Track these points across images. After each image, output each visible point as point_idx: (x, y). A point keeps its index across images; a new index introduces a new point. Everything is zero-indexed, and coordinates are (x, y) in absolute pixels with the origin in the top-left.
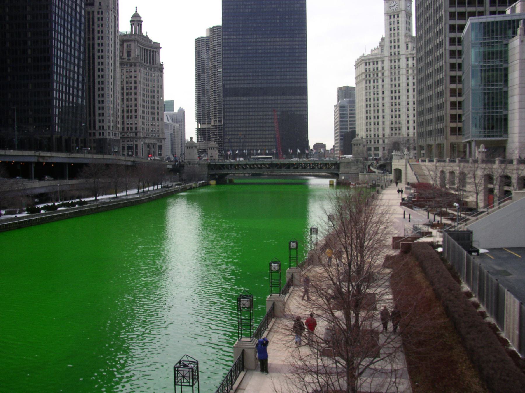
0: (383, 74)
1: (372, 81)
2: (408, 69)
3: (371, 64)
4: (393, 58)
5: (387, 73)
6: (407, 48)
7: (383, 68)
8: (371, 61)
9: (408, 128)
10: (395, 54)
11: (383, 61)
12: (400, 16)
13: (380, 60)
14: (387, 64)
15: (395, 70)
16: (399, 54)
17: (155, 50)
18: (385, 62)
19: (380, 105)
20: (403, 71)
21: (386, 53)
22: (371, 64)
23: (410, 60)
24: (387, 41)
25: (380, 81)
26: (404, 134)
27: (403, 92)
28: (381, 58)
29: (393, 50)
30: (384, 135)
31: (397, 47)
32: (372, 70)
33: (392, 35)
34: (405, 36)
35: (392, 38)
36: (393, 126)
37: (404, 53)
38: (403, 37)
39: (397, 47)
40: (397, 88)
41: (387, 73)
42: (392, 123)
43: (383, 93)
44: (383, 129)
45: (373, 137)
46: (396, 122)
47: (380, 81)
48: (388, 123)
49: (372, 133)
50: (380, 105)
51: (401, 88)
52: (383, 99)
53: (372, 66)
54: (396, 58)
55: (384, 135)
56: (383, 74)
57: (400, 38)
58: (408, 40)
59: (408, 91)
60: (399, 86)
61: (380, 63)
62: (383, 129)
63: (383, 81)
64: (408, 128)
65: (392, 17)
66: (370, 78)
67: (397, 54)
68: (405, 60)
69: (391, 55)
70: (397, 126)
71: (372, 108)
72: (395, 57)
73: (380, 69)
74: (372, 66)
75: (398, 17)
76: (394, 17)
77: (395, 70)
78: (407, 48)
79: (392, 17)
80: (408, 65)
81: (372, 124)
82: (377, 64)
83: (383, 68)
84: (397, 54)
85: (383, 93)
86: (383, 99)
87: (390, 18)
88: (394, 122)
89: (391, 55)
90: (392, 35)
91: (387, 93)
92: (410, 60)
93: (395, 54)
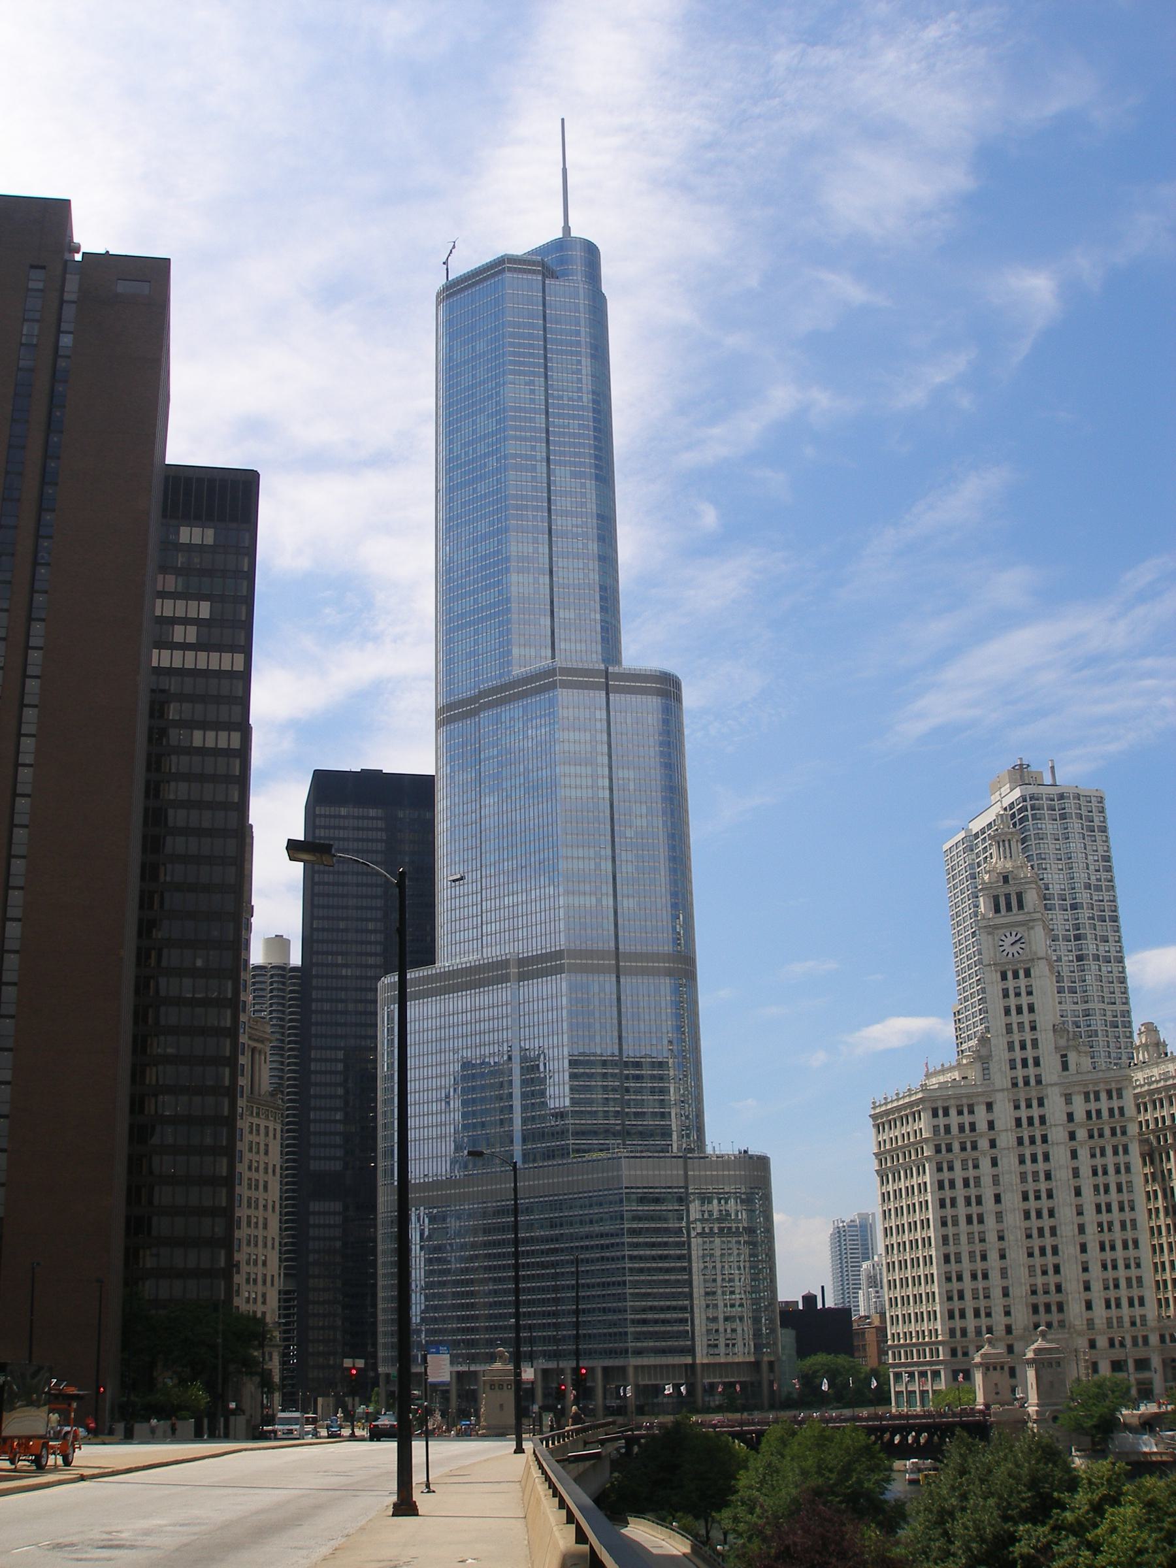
2: (1071, 1127)
3: (953, 1112)
5: (1006, 1139)
6: (1065, 1067)
9: (1089, 1306)
10: (1027, 1083)
11: (989, 1106)
14: (1004, 1114)
15: (1032, 1134)
17: (259, 1045)
20: (1058, 1134)
21: (1001, 1077)
23: (1078, 1100)
24: (999, 1044)
25: (985, 1163)
26: (1077, 1323)
27: (1064, 1201)
29: (1020, 1072)
30: (1009, 1330)
31: (1030, 1062)
33: (1015, 1027)
34: (1054, 1031)
35: (1016, 1038)
36: (1041, 1299)
37: (1054, 1078)
39: (1030, 1062)
40: (1043, 1186)
41: (1006, 1139)
42: (1034, 1292)
43: (998, 1199)
47: (985, 1163)
48: (1020, 1291)
51: (1052, 1184)
52: (999, 1216)
53: (954, 1120)
54: (1034, 1094)
56: (993, 1144)
58: (1062, 1042)
59: (1078, 1193)
60: (1048, 1176)
61: (981, 1110)
63: (994, 1163)
64: (1089, 1306)
65: (1010, 975)
67: (1033, 1082)
69: (1015, 1085)
70: (1054, 1298)
71: (965, 1249)
72: (1028, 1090)
73: (982, 1126)
74: (954, 1120)
75: (1028, 974)
76: (1016, 976)
77: (1032, 1134)
78: (1065, 1067)
79: (1010, 975)
80: (1070, 1117)
84: (1033, 1082)
85: (998, 1199)
86: (999, 1216)
87: (1004, 977)
89: (1015, 1085)
90: (1015, 1027)
91: (1012, 1200)
92: (1078, 1100)
93: (1027, 1083)
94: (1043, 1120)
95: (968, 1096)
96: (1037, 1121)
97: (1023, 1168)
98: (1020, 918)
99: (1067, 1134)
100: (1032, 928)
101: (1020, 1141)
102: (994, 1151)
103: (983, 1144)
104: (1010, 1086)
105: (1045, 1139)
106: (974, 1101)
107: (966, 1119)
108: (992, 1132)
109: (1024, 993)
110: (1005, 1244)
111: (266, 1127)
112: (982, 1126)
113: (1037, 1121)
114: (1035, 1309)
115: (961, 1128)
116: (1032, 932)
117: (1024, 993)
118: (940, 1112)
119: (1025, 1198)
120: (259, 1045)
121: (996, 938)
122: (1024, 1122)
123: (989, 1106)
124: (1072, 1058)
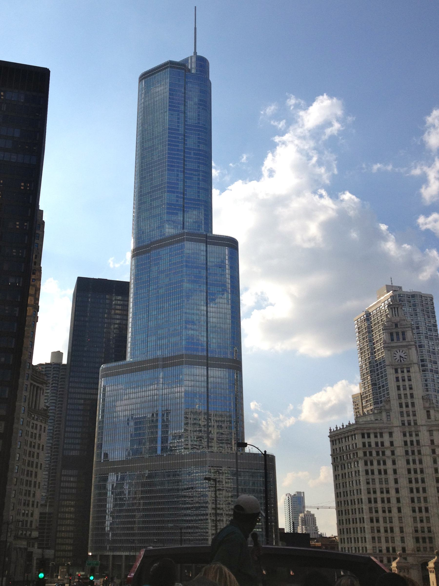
0: (393, 453)
1: (375, 463)
3: (372, 436)
4: (407, 430)
5: (400, 451)
7: (392, 443)
8: (372, 431)
10: (409, 424)
11: (391, 434)
12: (412, 370)
13: (386, 430)
14: (398, 439)
16: (416, 424)
17: (40, 386)
18: (394, 435)
19: (393, 501)
22: (372, 436)
25: (389, 463)
28: (387, 428)
32: (373, 445)
36: (420, 535)
37: (424, 423)
38: (421, 401)
41: (400, 451)
42: (416, 531)
44: (403, 540)
45: (384, 551)
46: (423, 528)
48: (409, 530)
49: (384, 546)
50: (393, 501)
53: (373, 440)
55: (404, 549)
56: (393, 453)
57: (416, 401)
60: (422, 471)
62: (403, 540)
63: (394, 463)
66: (371, 458)
67: (412, 424)
68: (427, 434)
69: (403, 424)
70: (426, 535)
73: (387, 444)
74: (373, 440)
81: (382, 530)
82: (381, 436)
83: (392, 443)
84: (412, 424)
87: (396, 371)
88: (419, 529)
89: (403, 424)
93: (409, 424)
94: (418, 442)
95: (381, 428)
96: (415, 443)
97: (409, 467)
98: (405, 344)
99: (431, 451)
100: (410, 349)
101: (407, 452)
102: (393, 457)
103: (388, 453)
104: (401, 425)
105: (419, 452)
106: (383, 431)
107: (379, 440)
108: (392, 447)
109: (406, 380)
110: (400, 505)
111: (41, 426)
112: (387, 444)
113: (415, 443)
114: (417, 540)
115: (377, 444)
116: (410, 351)
117: (406, 380)
118: (366, 436)
119: (410, 482)
120: (40, 386)
121: (392, 353)
122: (409, 443)
123: (391, 434)
124: (432, 412)
